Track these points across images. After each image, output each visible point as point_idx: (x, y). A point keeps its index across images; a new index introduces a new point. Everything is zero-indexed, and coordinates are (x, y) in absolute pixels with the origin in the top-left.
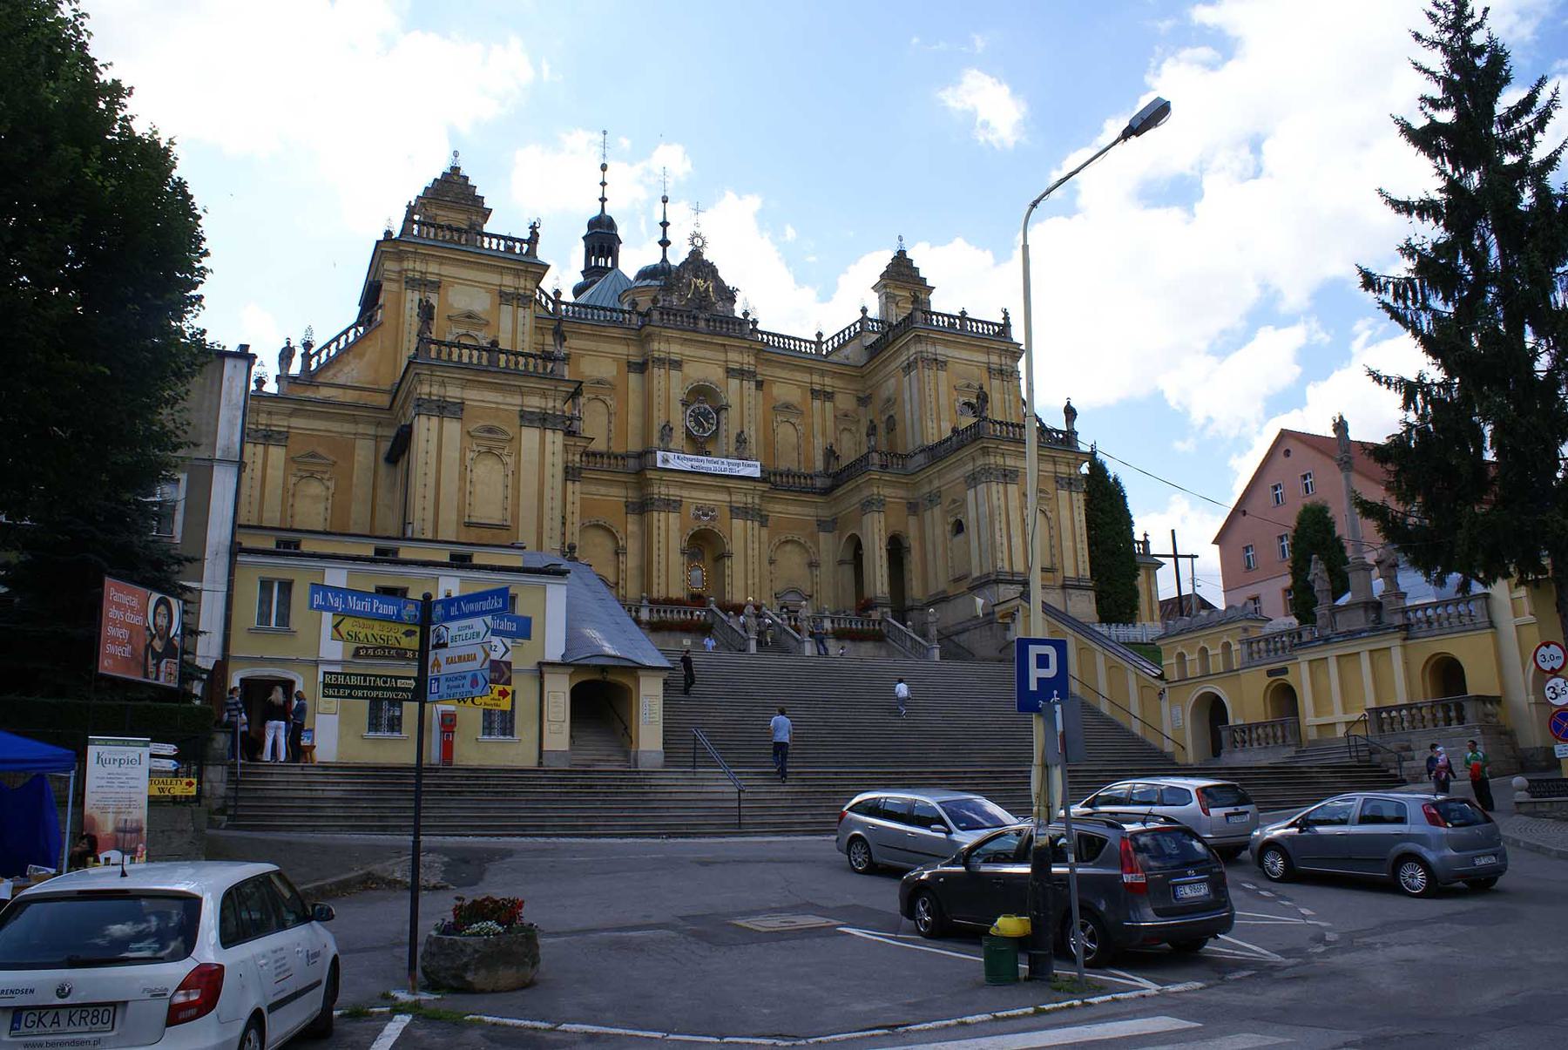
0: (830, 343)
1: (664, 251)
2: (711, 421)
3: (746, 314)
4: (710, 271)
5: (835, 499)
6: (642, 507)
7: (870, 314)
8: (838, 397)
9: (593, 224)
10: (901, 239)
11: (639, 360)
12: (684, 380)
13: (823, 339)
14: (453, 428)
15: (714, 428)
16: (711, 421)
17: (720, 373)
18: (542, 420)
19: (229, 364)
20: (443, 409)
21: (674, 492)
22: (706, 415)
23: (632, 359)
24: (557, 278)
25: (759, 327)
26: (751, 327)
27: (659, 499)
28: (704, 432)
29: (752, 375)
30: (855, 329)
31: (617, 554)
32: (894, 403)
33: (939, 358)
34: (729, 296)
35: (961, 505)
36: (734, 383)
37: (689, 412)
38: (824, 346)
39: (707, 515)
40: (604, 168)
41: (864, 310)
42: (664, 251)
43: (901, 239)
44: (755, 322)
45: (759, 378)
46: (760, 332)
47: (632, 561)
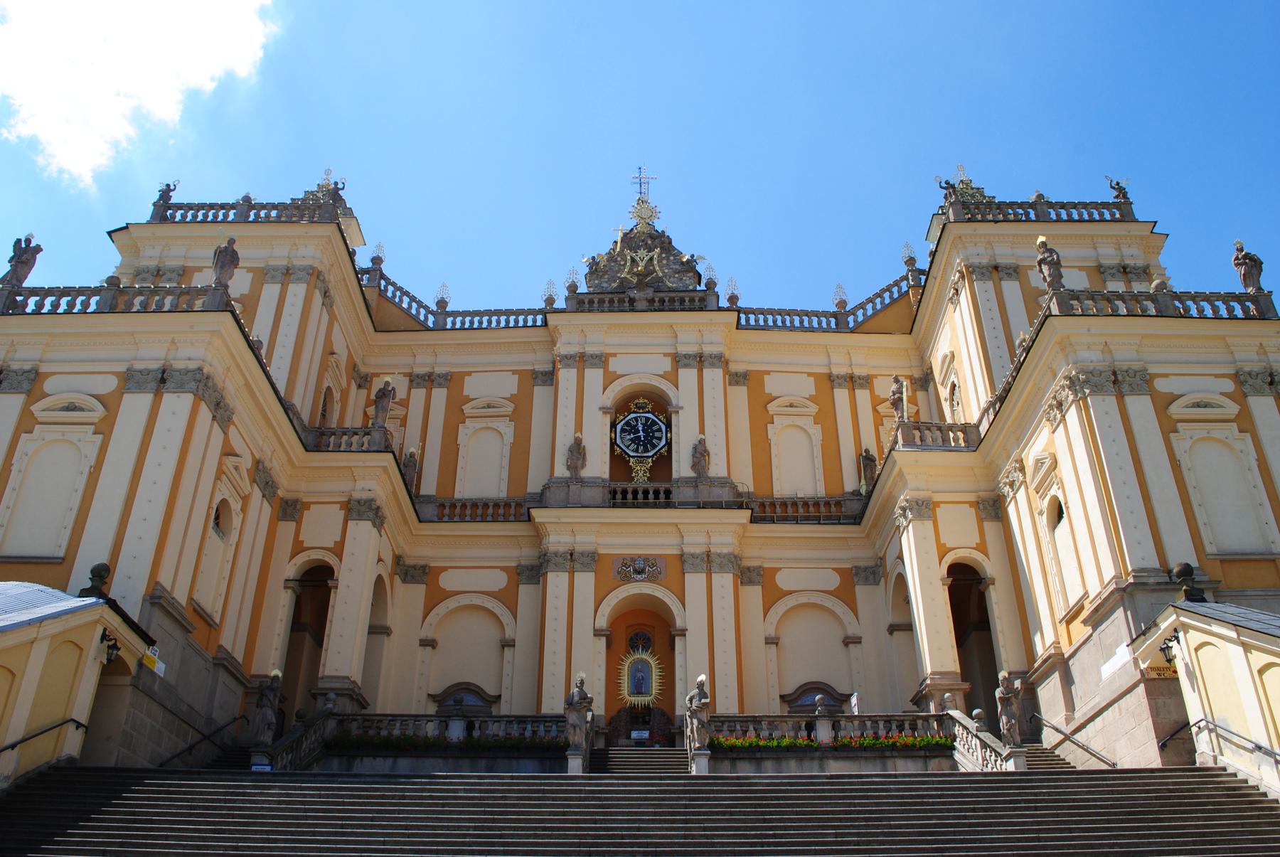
0: (860, 313)
2: (657, 434)
3: (711, 285)
4: (662, 242)
5: (874, 525)
6: (534, 572)
7: (918, 265)
11: (548, 367)
12: (610, 379)
13: (848, 308)
15: (663, 442)
16: (657, 434)
17: (667, 365)
21: (585, 541)
22: (649, 426)
24: (444, 285)
25: (741, 304)
26: (724, 303)
27: (556, 554)
28: (646, 450)
29: (720, 360)
30: (900, 289)
31: (503, 646)
32: (953, 356)
34: (690, 267)
35: (1055, 464)
36: (688, 376)
37: (619, 427)
38: (851, 319)
41: (911, 261)
44: (733, 299)
45: (733, 367)
46: (739, 311)
47: (518, 659)
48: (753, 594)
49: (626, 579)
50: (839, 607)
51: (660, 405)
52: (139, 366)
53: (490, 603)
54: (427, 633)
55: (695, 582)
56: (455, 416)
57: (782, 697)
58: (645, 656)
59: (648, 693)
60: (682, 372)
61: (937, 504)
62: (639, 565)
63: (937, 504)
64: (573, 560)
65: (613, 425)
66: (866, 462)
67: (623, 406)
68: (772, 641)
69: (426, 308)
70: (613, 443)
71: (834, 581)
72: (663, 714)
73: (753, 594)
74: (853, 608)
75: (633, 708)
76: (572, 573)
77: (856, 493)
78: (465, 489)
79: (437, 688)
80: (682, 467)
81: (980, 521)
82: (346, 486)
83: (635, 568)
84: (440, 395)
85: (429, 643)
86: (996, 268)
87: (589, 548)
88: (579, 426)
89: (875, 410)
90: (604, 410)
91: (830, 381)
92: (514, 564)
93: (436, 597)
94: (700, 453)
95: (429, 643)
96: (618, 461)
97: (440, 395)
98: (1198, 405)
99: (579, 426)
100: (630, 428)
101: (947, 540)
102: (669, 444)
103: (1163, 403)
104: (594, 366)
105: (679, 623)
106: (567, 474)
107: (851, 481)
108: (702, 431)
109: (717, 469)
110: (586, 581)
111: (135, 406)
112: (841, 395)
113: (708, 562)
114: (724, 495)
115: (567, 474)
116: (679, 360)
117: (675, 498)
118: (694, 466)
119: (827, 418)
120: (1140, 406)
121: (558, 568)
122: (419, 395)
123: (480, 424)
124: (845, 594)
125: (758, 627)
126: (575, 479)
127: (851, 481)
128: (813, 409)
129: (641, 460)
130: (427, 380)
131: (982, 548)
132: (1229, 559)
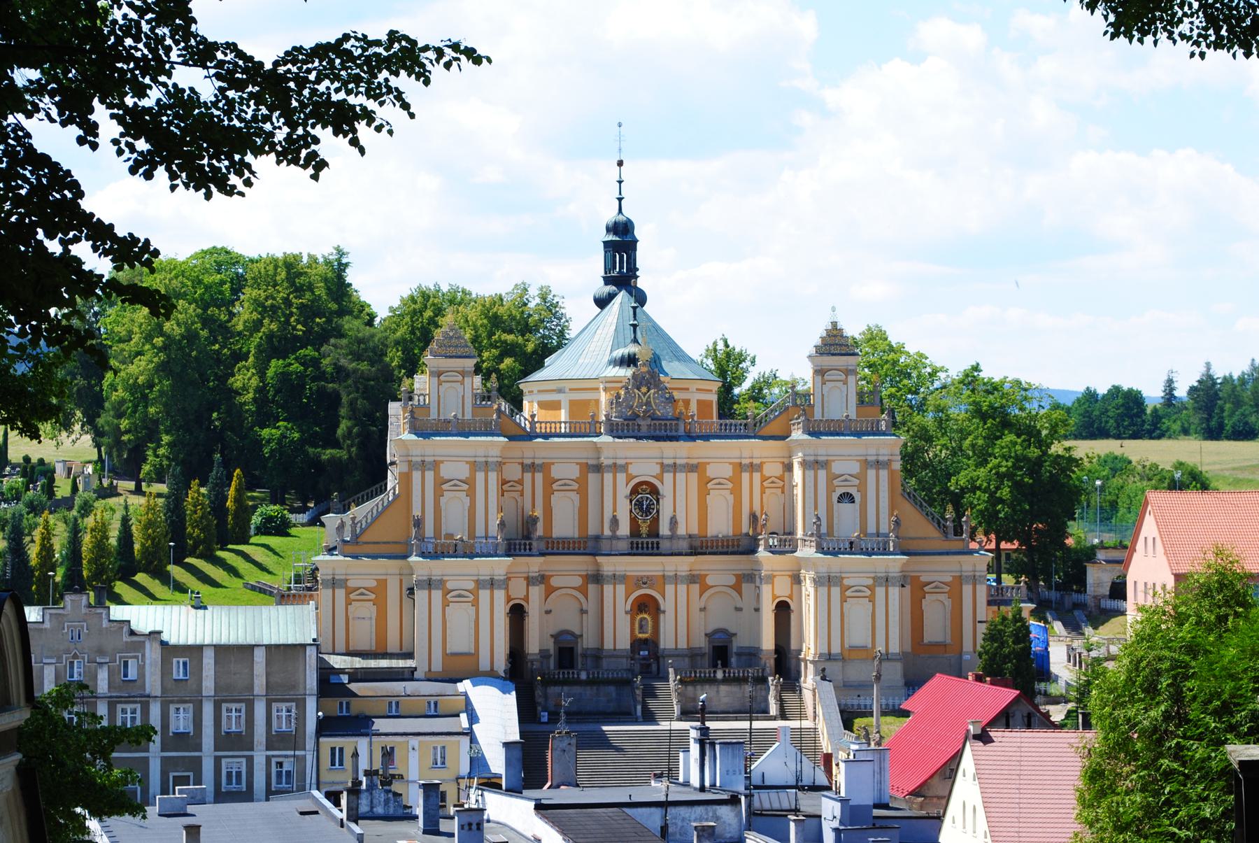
1: (635, 332)
6: (597, 578)
8: (765, 467)
10: (834, 309)
12: (630, 478)
14: (437, 595)
17: (657, 470)
18: (492, 584)
19: (308, 648)
20: (429, 584)
23: (591, 462)
27: (607, 576)
33: (820, 458)
36: (668, 477)
39: (645, 583)
40: (620, 163)
42: (635, 332)
43: (834, 309)
47: (590, 620)
48: (695, 588)
50: (734, 594)
51: (655, 491)
52: (481, 578)
54: (548, 607)
55: (670, 589)
56: (548, 493)
57: (706, 635)
58: (646, 616)
59: (646, 633)
60: (666, 475)
61: (775, 576)
62: (645, 580)
63: (775, 576)
64: (615, 579)
65: (631, 501)
66: (754, 518)
67: (634, 491)
68: (703, 609)
69: (525, 419)
70: (631, 511)
71: (732, 581)
72: (653, 642)
73: (695, 588)
74: (740, 594)
75: (640, 640)
76: (615, 584)
77: (747, 534)
79: (553, 632)
80: (664, 529)
81: (792, 584)
83: (643, 581)
84: (539, 477)
85: (548, 612)
87: (623, 573)
88: (615, 510)
89: (762, 485)
90: (626, 497)
91: (740, 468)
92: (585, 573)
93: (550, 591)
94: (674, 522)
95: (548, 612)
96: (633, 521)
97: (539, 477)
98: (856, 591)
99: (615, 510)
100: (639, 504)
101: (777, 593)
102: (658, 511)
103: (845, 589)
104: (621, 471)
105: (662, 608)
106: (610, 534)
107: (745, 528)
108: (675, 511)
109: (681, 531)
110: (621, 589)
111: (484, 595)
112: (746, 476)
113: (676, 579)
114: (684, 545)
115: (610, 534)
116: (664, 468)
117: (662, 550)
118: (670, 530)
119: (736, 491)
120: (836, 591)
121: (608, 583)
122: (528, 476)
124: (737, 588)
125: (697, 604)
126: (614, 537)
127: (745, 528)
128: (730, 485)
129: (644, 521)
130: (531, 468)
131: (790, 597)
132: (852, 648)
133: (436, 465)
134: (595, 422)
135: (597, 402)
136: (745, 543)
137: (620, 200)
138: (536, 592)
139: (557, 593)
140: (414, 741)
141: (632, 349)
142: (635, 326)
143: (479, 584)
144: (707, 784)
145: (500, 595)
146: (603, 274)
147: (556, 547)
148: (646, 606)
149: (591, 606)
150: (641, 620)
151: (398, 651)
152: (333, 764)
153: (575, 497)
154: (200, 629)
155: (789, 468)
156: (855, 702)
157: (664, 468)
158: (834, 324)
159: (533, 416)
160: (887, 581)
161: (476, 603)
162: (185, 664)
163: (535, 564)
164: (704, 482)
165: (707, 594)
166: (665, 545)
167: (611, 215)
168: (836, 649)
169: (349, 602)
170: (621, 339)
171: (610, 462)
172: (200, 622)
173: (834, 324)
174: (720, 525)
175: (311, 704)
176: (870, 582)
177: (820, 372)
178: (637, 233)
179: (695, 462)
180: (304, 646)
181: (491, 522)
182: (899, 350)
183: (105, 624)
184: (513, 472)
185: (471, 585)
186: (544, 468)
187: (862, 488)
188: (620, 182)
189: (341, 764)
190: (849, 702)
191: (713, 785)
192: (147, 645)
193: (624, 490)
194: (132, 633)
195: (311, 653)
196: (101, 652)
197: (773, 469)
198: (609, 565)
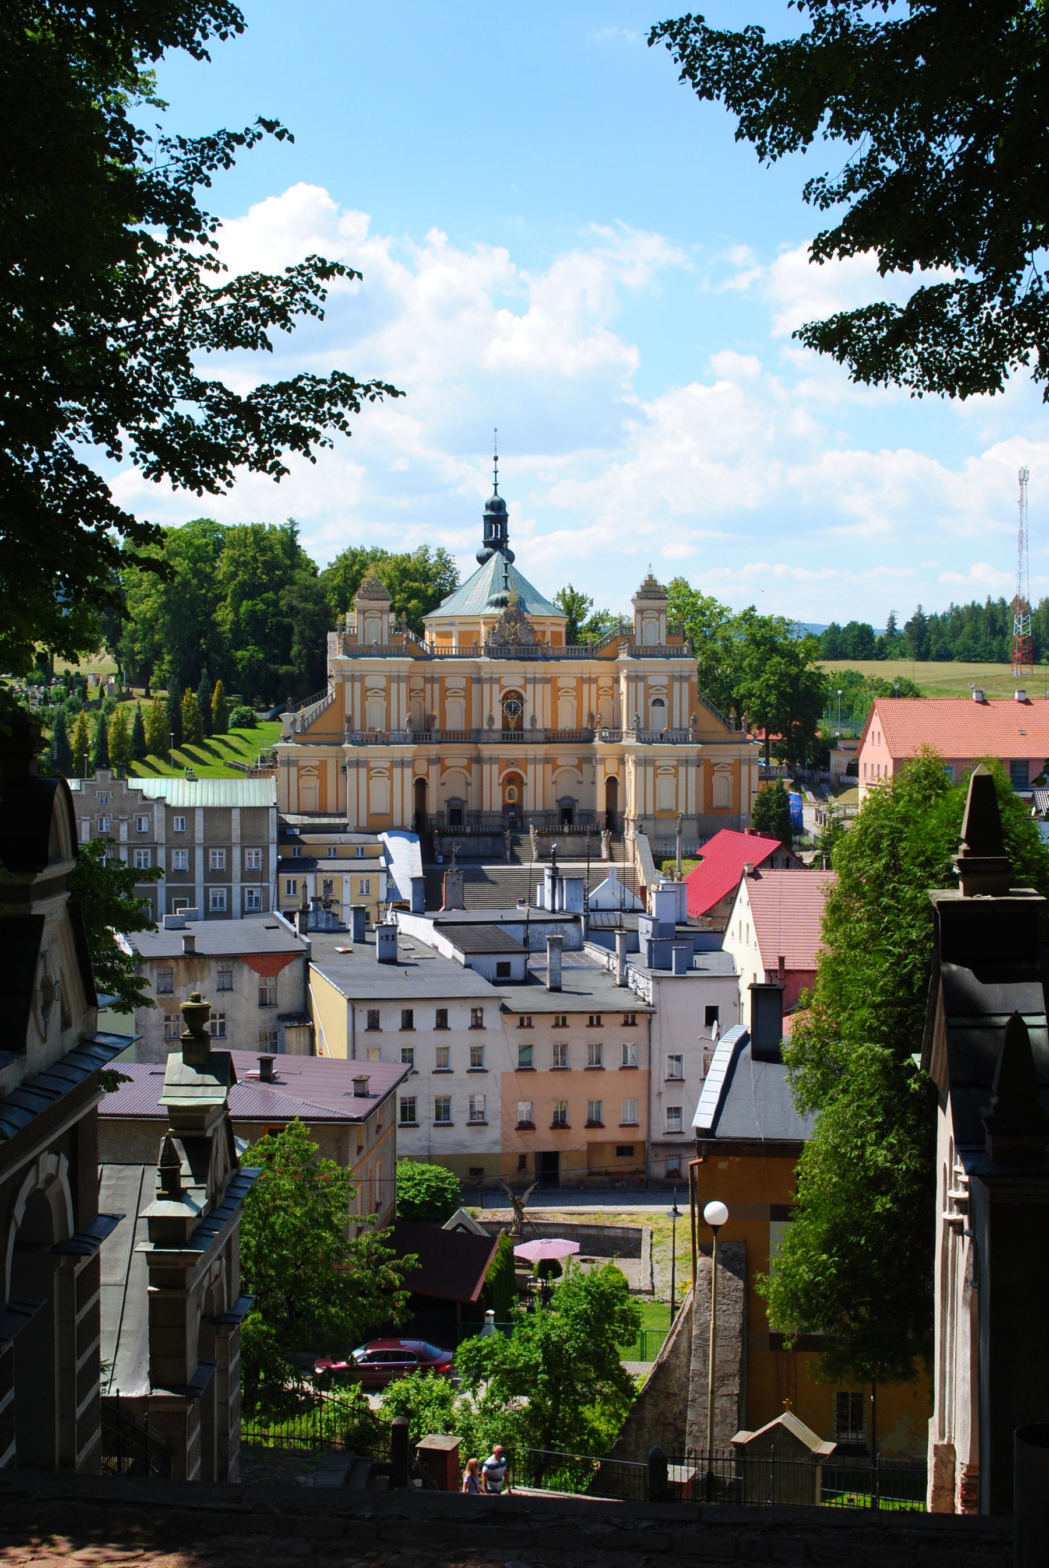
6: (478, 760)
9: (491, 506)
10: (650, 566)
12: (502, 688)
14: (363, 771)
17: (522, 682)
18: (402, 764)
20: (357, 764)
23: (474, 676)
36: (530, 687)
40: (496, 459)
43: (650, 566)
47: (473, 789)
48: (549, 767)
49: (509, 767)
51: (520, 697)
53: (463, 770)
55: (530, 768)
64: (491, 760)
66: (591, 717)
67: (506, 697)
71: (576, 762)
73: (549, 767)
74: (581, 772)
77: (586, 729)
78: (449, 726)
79: (447, 798)
80: (527, 725)
82: (426, 753)
83: (511, 762)
84: (436, 686)
85: (443, 784)
86: (637, 676)
88: (491, 711)
91: (581, 680)
93: (444, 769)
94: (534, 719)
95: (443, 784)
96: (505, 718)
97: (436, 686)
99: (491, 711)
100: (509, 707)
107: (585, 724)
109: (539, 726)
110: (495, 768)
111: (397, 771)
112: (586, 687)
113: (535, 761)
116: (527, 680)
119: (579, 698)
120: (650, 770)
122: (428, 686)
123: (453, 699)
124: (579, 767)
125: (550, 778)
126: (491, 730)
127: (585, 724)
128: (575, 693)
129: (513, 719)
130: (431, 680)
131: (617, 774)
132: (662, 811)
133: (362, 678)
134: (477, 646)
135: (479, 632)
136: (585, 735)
137: (496, 485)
138: (434, 770)
139: (449, 771)
140: (347, 876)
141: (504, 594)
142: (506, 578)
143: (394, 764)
144: (557, 908)
145: (408, 772)
146: (482, 538)
147: (448, 738)
148: (514, 780)
149: (474, 780)
150: (510, 790)
151: (335, 811)
152: (289, 892)
153: (463, 701)
154: (193, 795)
155: (617, 681)
156: (664, 849)
157: (527, 680)
158: (651, 576)
159: (432, 643)
160: (687, 762)
161: (391, 778)
162: (182, 820)
163: (433, 750)
164: (556, 691)
165: (557, 771)
166: (527, 736)
167: (488, 496)
168: (650, 811)
169: (299, 777)
170: (496, 587)
171: (488, 676)
172: (193, 790)
173: (651, 576)
174: (567, 722)
175: (273, 850)
176: (675, 763)
177: (640, 611)
178: (508, 510)
179: (549, 676)
180: (267, 808)
181: (402, 719)
182: (696, 595)
183: (125, 792)
184: (418, 683)
185: (388, 765)
186: (441, 680)
187: (670, 696)
188: (496, 472)
189: (294, 892)
190: (659, 849)
191: (561, 909)
192: (155, 807)
193: (498, 696)
194: (144, 798)
195: (273, 813)
196: (122, 811)
197: (605, 682)
198: (487, 750)
